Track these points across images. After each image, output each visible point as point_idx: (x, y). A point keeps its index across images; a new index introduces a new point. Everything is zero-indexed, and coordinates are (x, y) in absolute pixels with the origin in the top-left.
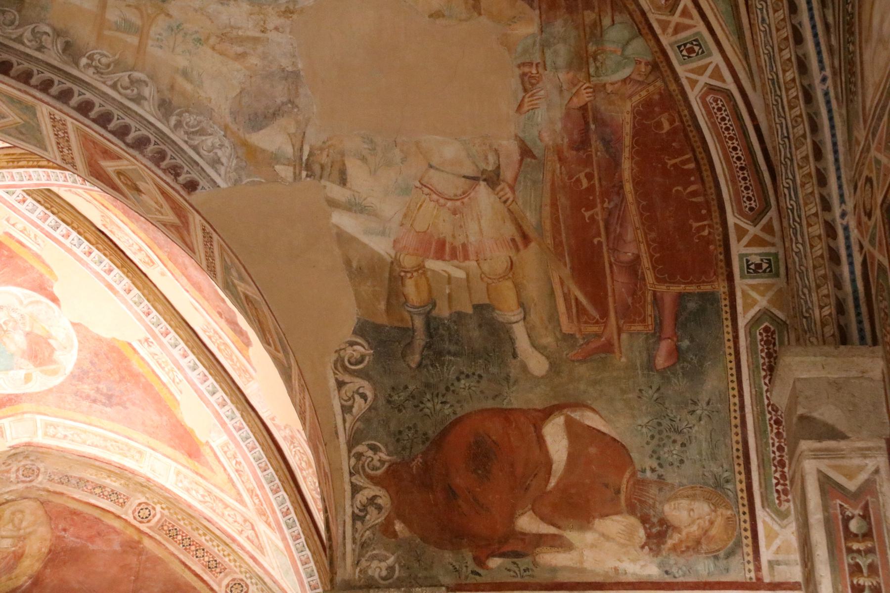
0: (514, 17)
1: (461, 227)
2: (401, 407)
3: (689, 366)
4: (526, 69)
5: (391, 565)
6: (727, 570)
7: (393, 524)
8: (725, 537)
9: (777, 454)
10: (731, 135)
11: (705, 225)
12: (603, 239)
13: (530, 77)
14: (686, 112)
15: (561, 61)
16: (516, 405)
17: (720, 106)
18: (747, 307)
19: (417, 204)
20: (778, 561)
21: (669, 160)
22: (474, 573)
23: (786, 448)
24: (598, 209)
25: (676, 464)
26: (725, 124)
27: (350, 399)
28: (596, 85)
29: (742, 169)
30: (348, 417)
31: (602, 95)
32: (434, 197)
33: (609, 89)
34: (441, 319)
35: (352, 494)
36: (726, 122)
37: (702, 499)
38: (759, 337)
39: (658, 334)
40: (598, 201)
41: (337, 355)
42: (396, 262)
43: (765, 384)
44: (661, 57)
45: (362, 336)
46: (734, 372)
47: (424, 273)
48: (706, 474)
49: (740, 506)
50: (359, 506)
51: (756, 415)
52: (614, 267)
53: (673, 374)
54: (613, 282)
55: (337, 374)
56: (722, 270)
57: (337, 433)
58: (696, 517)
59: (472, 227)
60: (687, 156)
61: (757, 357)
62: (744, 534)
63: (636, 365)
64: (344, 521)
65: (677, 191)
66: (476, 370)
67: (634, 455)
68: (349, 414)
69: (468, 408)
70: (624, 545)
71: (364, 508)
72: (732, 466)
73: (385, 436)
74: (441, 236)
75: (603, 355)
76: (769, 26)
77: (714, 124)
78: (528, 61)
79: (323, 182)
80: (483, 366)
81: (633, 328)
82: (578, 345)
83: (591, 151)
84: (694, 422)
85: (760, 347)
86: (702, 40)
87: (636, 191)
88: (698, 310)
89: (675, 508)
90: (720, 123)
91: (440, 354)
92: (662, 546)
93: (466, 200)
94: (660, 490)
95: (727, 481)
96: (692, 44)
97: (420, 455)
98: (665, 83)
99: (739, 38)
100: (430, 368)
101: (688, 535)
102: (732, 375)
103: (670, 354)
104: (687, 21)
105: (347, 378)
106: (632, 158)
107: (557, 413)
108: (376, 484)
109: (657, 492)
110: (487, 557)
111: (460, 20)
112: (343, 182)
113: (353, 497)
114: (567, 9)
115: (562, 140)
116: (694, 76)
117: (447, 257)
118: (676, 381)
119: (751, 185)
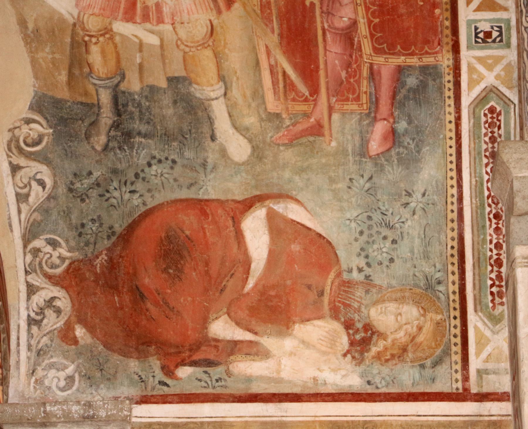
2: (84, 197)
3: (406, 152)
5: (71, 374)
6: (433, 380)
7: (73, 330)
8: (433, 344)
9: (495, 252)
16: (213, 196)
18: (472, 84)
20: (487, 369)
23: (504, 245)
25: (386, 263)
27: (25, 186)
30: (24, 207)
34: (130, 94)
35: (28, 296)
37: (411, 302)
38: (483, 119)
39: (373, 115)
43: (487, 173)
45: (40, 111)
46: (454, 158)
47: (112, 38)
48: (417, 274)
49: (452, 310)
50: (35, 309)
51: (474, 209)
52: (328, 33)
53: (387, 160)
54: (325, 53)
55: (11, 157)
56: (448, 40)
57: (10, 226)
58: (404, 322)
61: (480, 142)
62: (453, 340)
63: (347, 150)
66: (169, 154)
67: (341, 253)
68: (24, 204)
69: (160, 198)
70: (324, 353)
71: (41, 312)
72: (445, 265)
73: (66, 230)
75: (311, 139)
80: (178, 150)
81: (346, 107)
82: (284, 126)
84: (408, 216)
88: (418, 86)
89: (381, 313)
91: (128, 135)
92: (366, 354)
94: (367, 292)
95: (439, 283)
100: (118, 151)
101: (393, 341)
102: (451, 162)
103: (385, 138)
105: (22, 161)
107: (258, 205)
108: (56, 284)
109: (363, 295)
110: (177, 366)
113: (29, 298)
118: (390, 169)
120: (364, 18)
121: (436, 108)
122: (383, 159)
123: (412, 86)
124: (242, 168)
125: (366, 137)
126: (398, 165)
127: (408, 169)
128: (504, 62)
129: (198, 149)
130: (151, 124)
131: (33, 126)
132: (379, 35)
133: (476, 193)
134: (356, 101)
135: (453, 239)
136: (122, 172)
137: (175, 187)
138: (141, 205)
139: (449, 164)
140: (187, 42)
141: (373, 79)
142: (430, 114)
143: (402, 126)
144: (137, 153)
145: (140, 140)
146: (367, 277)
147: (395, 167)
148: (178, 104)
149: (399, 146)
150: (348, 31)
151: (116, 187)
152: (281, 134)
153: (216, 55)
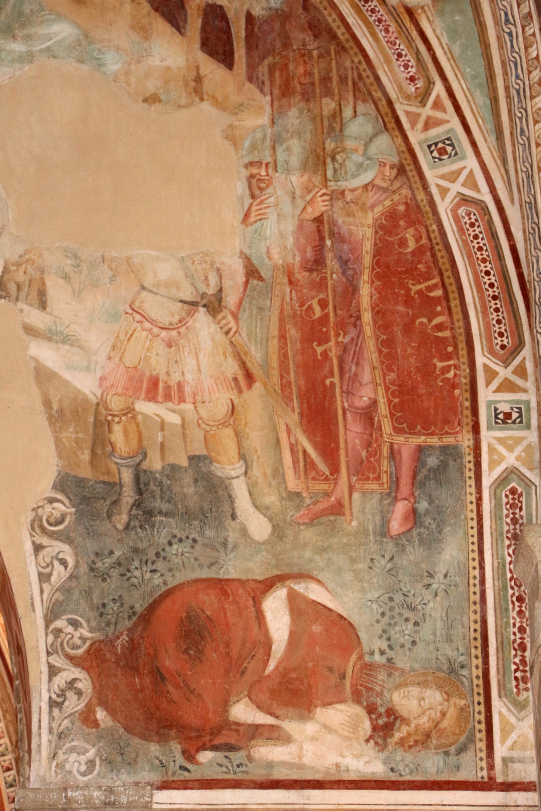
0: (242, 105)
1: (176, 362)
2: (105, 576)
4: (255, 171)
5: (92, 758)
6: (458, 768)
7: (94, 712)
8: (457, 731)
9: (518, 635)
10: (485, 256)
11: (451, 366)
12: (336, 380)
13: (259, 180)
14: (434, 227)
15: (295, 161)
16: (233, 575)
17: (473, 220)
18: (493, 464)
19: (127, 333)
20: (512, 758)
21: (414, 285)
22: (182, 768)
23: (528, 629)
24: (332, 343)
25: (408, 645)
26: (478, 243)
27: (48, 566)
28: (333, 192)
29: (495, 298)
30: (46, 586)
31: (340, 204)
32: (147, 325)
33: (349, 197)
34: (151, 472)
35: (49, 677)
36: (480, 240)
37: (434, 687)
38: (505, 500)
39: (393, 494)
40: (332, 333)
41: (34, 513)
42: (102, 403)
43: (509, 555)
44: (409, 158)
46: (475, 539)
47: (134, 418)
48: (440, 657)
49: (475, 695)
50: (56, 691)
51: (497, 591)
52: (348, 412)
53: (408, 541)
55: (34, 536)
56: (468, 420)
57: (33, 605)
58: (427, 707)
59: (190, 363)
60: (433, 282)
61: (502, 523)
62: (478, 726)
63: (368, 530)
64: (40, 708)
65: (421, 323)
66: (190, 533)
67: (363, 635)
68: (47, 584)
69: (180, 578)
70: (347, 738)
71: (62, 693)
72: (468, 649)
73: (87, 609)
74: (154, 373)
75: (332, 518)
76: (528, 139)
77: (465, 242)
78: (256, 159)
79: (21, 305)
80: (199, 529)
81: (366, 486)
82: (305, 505)
83: (326, 273)
84: (430, 597)
85: (505, 512)
86: (455, 139)
87: (375, 322)
88: (439, 466)
89: (404, 697)
90: (472, 242)
91: (150, 514)
92: (389, 740)
93: (183, 330)
94: (390, 675)
95: (463, 667)
96: (444, 143)
97: (126, 633)
98: (413, 194)
99: (497, 139)
100: (139, 530)
101: (417, 726)
102: (473, 543)
103: (406, 518)
104: (440, 115)
105: (45, 541)
106: (373, 282)
107: (278, 585)
108: (77, 665)
109: (385, 679)
110: (197, 751)
111: (180, 107)
112: (43, 305)
113: (50, 680)
114: (303, 95)
115: (294, 259)
116: (445, 184)
117: (160, 398)
118: (411, 550)
119: (503, 318)
120: (383, 398)
121: (457, 488)
122: (404, 539)
123: (433, 465)
124: (263, 547)
125: (387, 517)
126: (420, 546)
127: (429, 549)
128: (525, 443)
129: (219, 528)
130: (172, 503)
131: (56, 505)
132: (399, 414)
133: (498, 575)
134: (376, 480)
135: (476, 622)
136: (143, 550)
137: (196, 565)
138: (162, 585)
139: (470, 545)
140: (208, 420)
141: (394, 459)
142: (451, 494)
143: (423, 506)
144: (158, 532)
145: (161, 519)
146: (389, 660)
147: (416, 548)
148: (199, 483)
149: (420, 526)
150: (368, 410)
151: (137, 566)
152: (301, 513)
153: (237, 434)
